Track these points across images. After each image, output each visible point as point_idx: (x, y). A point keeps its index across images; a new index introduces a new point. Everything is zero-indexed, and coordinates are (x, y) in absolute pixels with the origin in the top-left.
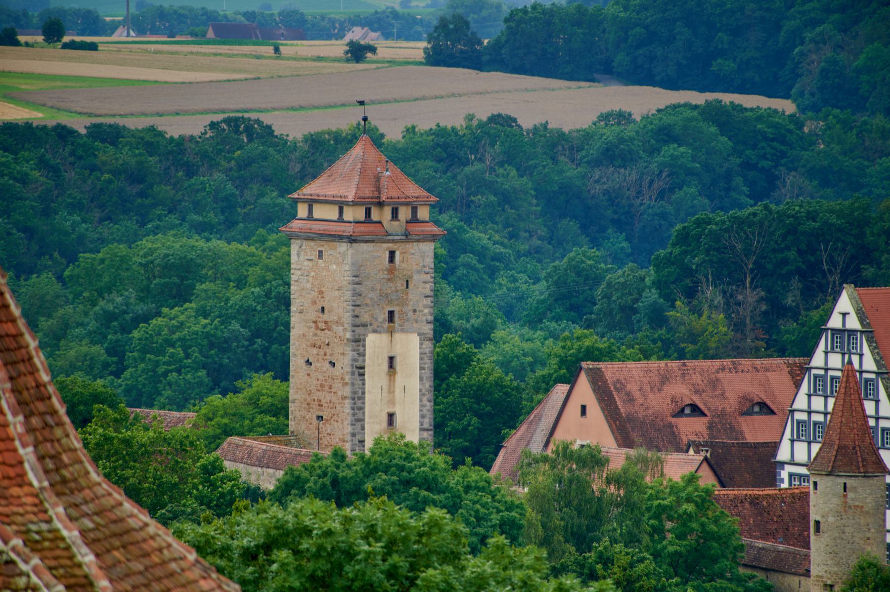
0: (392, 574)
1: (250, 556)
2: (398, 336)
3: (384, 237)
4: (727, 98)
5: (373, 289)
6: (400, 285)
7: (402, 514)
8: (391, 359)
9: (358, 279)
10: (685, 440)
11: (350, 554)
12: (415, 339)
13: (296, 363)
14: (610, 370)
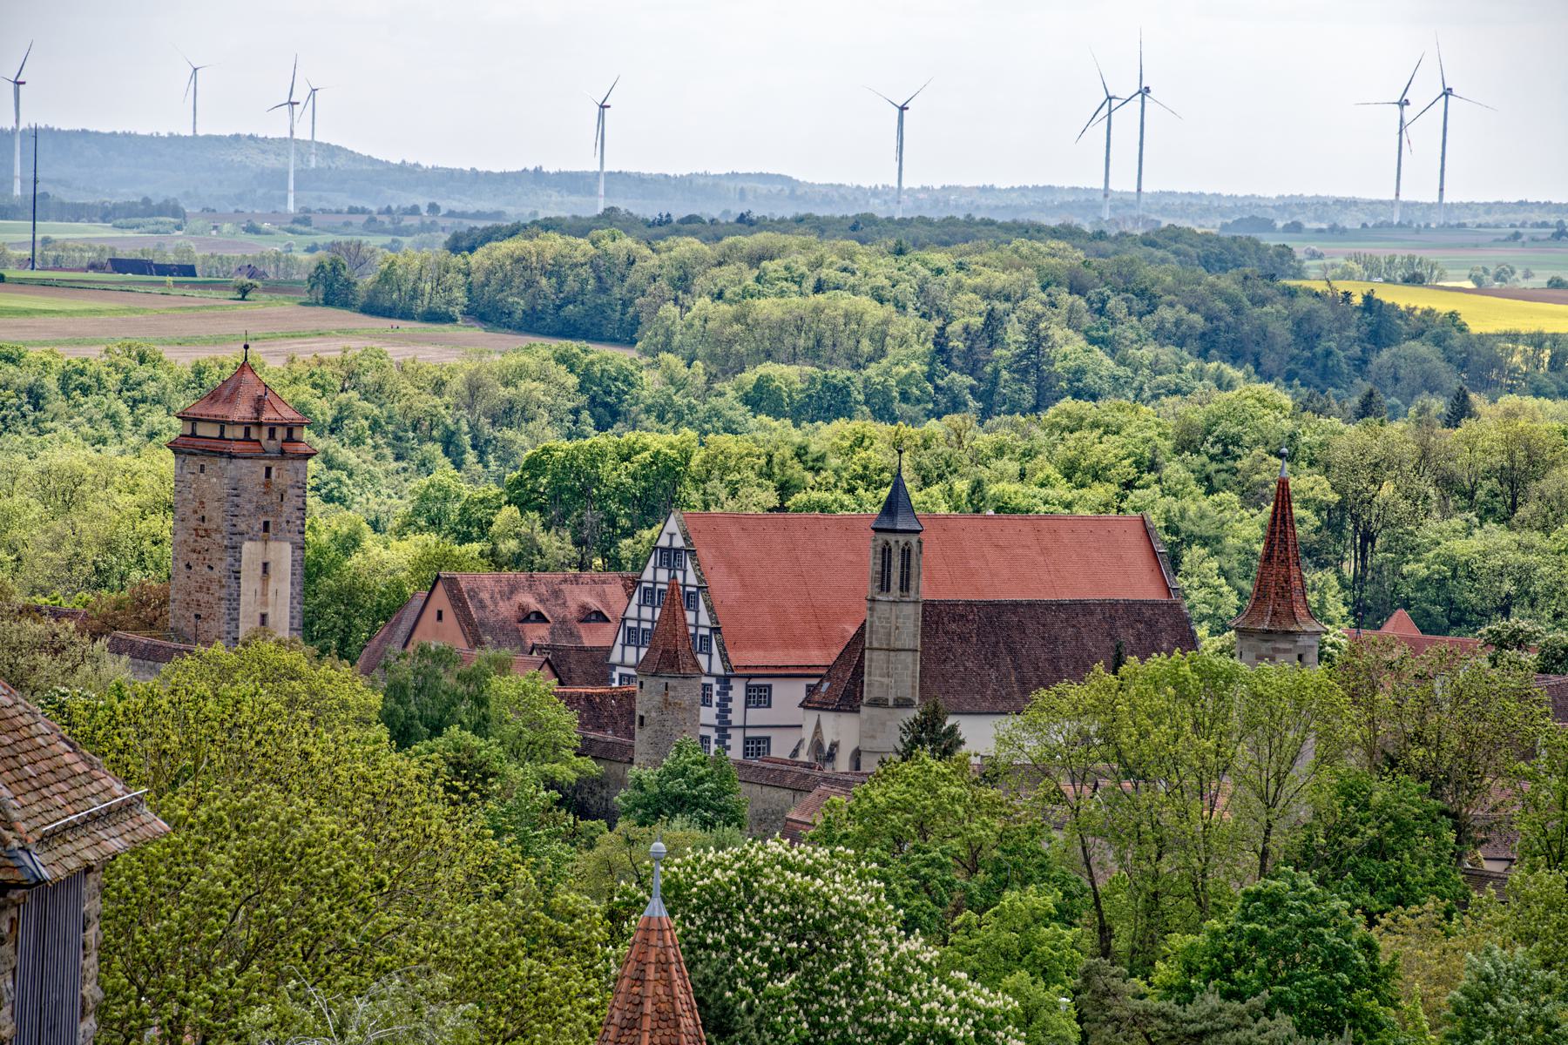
2: (272, 544)
5: (250, 501)
6: (275, 497)
8: (265, 565)
10: (529, 643)
12: (288, 547)
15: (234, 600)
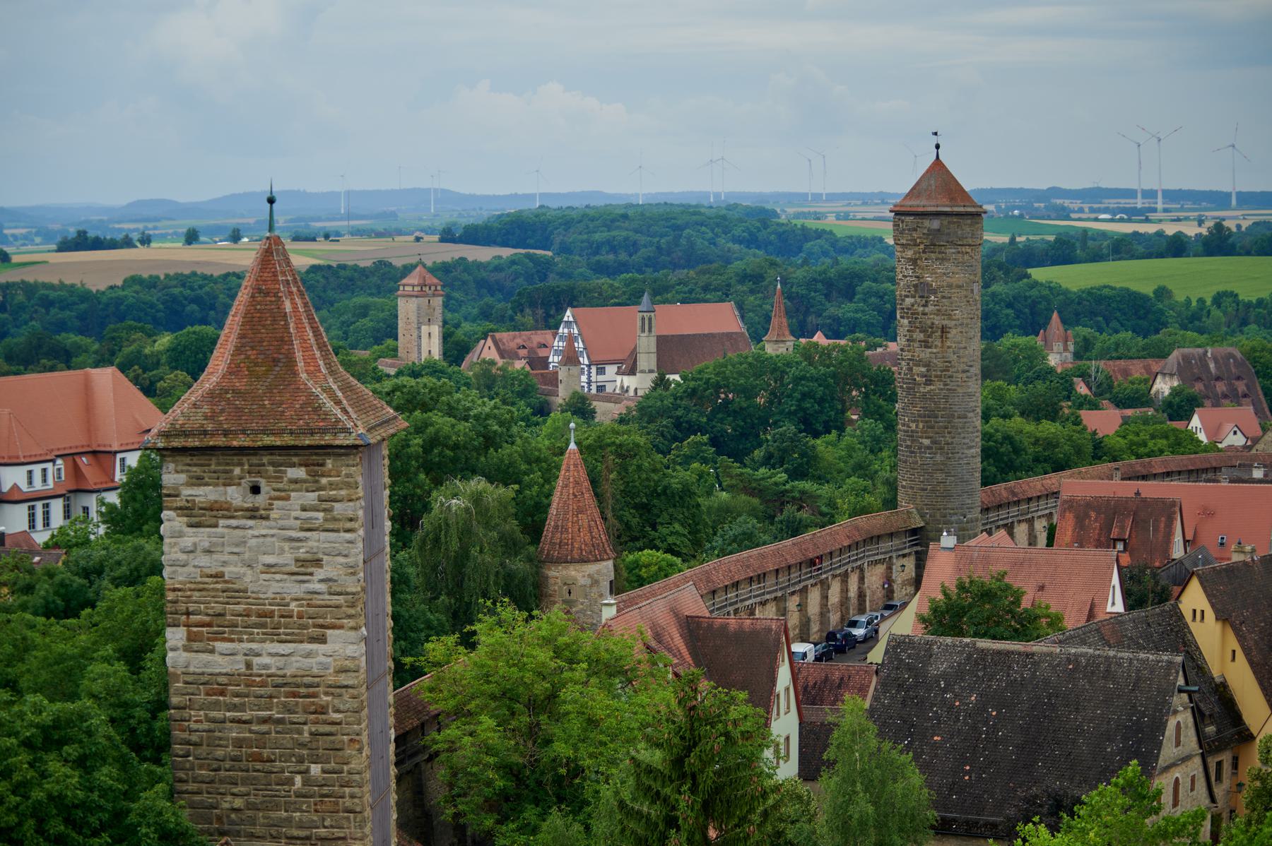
0: (431, 399)
1: (388, 394)
3: (427, 296)
4: (531, 251)
7: (434, 380)
9: (419, 308)
11: (418, 393)
13: (400, 335)
14: (497, 335)
15: (419, 346)
